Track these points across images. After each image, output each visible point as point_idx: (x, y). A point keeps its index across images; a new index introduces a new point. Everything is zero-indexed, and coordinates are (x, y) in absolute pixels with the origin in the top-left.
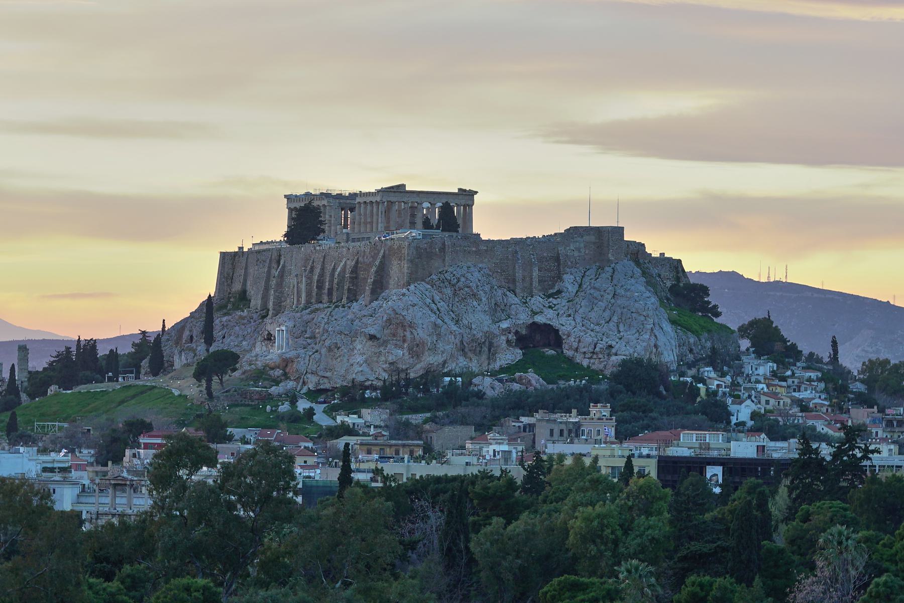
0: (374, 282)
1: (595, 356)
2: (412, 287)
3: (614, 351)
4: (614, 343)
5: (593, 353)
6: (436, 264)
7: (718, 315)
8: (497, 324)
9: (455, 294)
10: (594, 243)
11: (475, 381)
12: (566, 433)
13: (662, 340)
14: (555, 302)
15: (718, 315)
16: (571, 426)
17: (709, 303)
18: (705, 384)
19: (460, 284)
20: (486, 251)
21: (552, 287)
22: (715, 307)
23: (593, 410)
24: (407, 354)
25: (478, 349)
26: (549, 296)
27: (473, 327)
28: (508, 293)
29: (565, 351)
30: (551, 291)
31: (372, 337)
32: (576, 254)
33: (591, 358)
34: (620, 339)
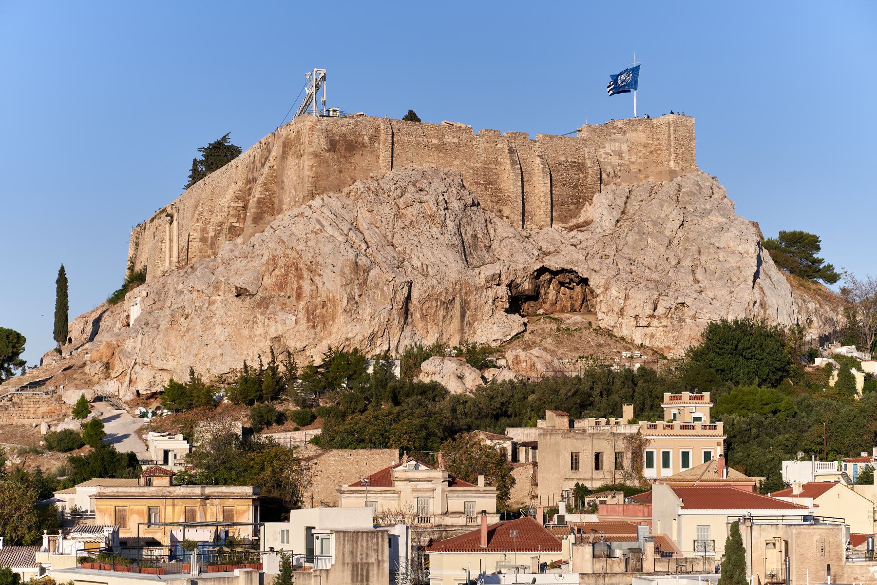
0: (259, 202)
1: (655, 323)
2: (317, 202)
3: (688, 313)
4: (688, 301)
5: (652, 316)
6: (365, 164)
7: (833, 278)
8: (477, 271)
9: (398, 216)
10: (645, 146)
11: (426, 366)
12: (608, 461)
13: (772, 300)
14: (581, 236)
15: (833, 278)
16: (621, 445)
17: (820, 261)
18: (860, 369)
19: (407, 195)
20: (458, 145)
21: (576, 215)
22: (829, 267)
23: (670, 407)
24: (303, 321)
25: (441, 313)
26: (571, 229)
27: (431, 271)
28: (497, 220)
29: (600, 316)
30: (574, 222)
31: (240, 293)
32: (615, 160)
33: (648, 326)
34: (700, 292)
